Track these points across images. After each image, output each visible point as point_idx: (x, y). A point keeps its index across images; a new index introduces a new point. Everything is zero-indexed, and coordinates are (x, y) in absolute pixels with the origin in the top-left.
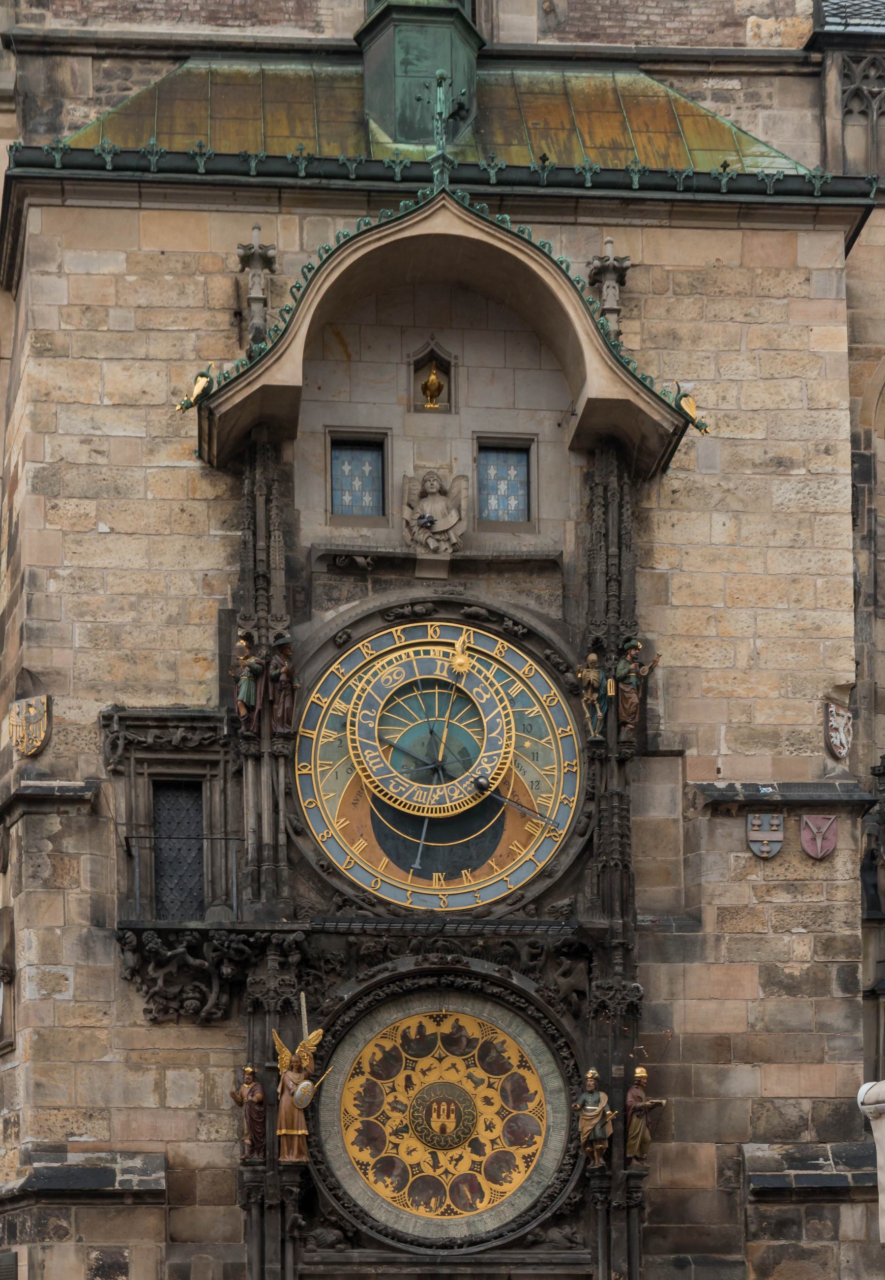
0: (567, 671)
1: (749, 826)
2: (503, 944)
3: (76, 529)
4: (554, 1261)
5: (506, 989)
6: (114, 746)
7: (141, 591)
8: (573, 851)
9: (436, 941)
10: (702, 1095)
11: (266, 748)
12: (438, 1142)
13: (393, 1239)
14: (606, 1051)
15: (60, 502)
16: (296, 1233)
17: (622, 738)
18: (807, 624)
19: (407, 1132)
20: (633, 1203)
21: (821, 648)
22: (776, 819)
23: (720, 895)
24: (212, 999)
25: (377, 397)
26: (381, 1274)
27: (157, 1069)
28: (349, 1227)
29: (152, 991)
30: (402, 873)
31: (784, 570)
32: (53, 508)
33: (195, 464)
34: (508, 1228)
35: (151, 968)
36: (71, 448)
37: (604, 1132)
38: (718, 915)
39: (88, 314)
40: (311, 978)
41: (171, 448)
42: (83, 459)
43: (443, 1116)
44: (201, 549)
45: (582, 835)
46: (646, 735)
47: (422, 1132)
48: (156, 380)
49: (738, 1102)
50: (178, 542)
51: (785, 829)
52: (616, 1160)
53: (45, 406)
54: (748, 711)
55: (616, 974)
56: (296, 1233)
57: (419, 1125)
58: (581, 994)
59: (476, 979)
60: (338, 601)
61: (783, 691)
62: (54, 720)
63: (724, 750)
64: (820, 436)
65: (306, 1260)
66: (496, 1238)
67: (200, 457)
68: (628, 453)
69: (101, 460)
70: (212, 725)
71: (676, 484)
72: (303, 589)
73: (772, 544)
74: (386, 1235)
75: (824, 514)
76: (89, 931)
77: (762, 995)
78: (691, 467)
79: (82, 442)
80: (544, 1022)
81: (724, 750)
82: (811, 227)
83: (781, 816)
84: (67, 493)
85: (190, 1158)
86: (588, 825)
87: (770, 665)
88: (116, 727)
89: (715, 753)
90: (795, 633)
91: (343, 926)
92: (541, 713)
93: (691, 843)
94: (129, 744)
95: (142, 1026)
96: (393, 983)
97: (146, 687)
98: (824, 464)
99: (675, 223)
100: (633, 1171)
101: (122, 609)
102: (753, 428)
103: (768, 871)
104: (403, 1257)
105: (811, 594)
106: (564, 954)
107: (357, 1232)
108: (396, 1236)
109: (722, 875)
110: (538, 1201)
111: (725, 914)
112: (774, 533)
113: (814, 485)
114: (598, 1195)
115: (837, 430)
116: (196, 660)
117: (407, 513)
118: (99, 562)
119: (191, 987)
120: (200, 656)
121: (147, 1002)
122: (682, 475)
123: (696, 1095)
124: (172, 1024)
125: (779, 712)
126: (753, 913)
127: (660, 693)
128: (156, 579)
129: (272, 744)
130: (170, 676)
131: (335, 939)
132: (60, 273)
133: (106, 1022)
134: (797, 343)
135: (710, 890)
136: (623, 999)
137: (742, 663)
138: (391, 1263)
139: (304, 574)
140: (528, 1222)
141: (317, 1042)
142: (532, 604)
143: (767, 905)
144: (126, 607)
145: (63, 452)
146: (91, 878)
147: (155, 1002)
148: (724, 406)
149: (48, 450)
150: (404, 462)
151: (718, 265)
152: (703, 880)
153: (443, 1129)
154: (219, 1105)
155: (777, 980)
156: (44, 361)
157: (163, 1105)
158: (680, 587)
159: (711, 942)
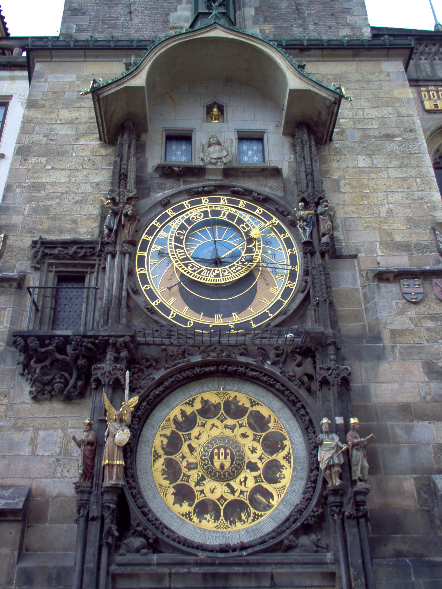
0: (288, 214)
1: (402, 286)
3: (36, 167)
4: (305, 561)
5: (261, 373)
6: (35, 256)
7: (63, 191)
8: (298, 301)
9: (216, 348)
12: (220, 476)
13: (184, 545)
15: (29, 158)
16: (110, 540)
17: (322, 252)
18: (416, 197)
19: (205, 479)
20: (360, 514)
22: (417, 282)
24: (72, 382)
25: (188, 117)
26: (175, 574)
27: (33, 430)
28: (150, 535)
30: (196, 314)
31: (398, 176)
32: (25, 160)
33: (97, 143)
34: (270, 536)
35: (32, 361)
38: (391, 334)
39: (56, 95)
40: (136, 370)
41: (87, 138)
42: (43, 142)
43: (222, 457)
44: (96, 174)
45: (303, 292)
46: (335, 249)
51: (424, 288)
53: (29, 125)
54: (390, 234)
55: (331, 360)
56: (110, 540)
57: (205, 464)
58: (310, 377)
59: (242, 367)
60: (164, 189)
61: (408, 226)
62: (7, 246)
63: (380, 253)
64: (406, 126)
65: (117, 562)
66: (261, 543)
67: (100, 139)
69: (52, 142)
70: (92, 246)
71: (337, 146)
72: (148, 188)
73: (390, 166)
74: (179, 542)
75: (415, 154)
76: (5, 349)
77: (426, 379)
79: (44, 136)
80: (287, 392)
81: (380, 253)
83: (420, 281)
85: (47, 489)
86: (306, 286)
87: (398, 215)
88: (38, 246)
89: (375, 255)
90: (410, 202)
91: (158, 340)
94: (45, 255)
95: (28, 403)
96: (188, 370)
97: (59, 230)
99: (324, 59)
101: (52, 198)
102: (372, 125)
103: (418, 310)
104: (191, 559)
106: (299, 353)
107: (157, 540)
108: (185, 542)
109: (390, 312)
110: (290, 515)
111: (394, 333)
112: (390, 162)
113: (407, 143)
114: (334, 508)
115: (414, 123)
116: (88, 219)
117: (201, 155)
118: (44, 180)
119: (59, 376)
121: (32, 387)
122: (341, 142)
124: (47, 402)
125: (408, 235)
127: (340, 229)
130: (73, 226)
131: (153, 347)
132: (46, 81)
133: (5, 401)
134: (388, 96)
135: (384, 321)
136: (338, 374)
137: (383, 215)
138: (182, 564)
140: (284, 531)
141: (134, 404)
142: (267, 190)
146: (11, 320)
147: (36, 386)
149: (27, 140)
150: (200, 138)
151: (346, 72)
152: (379, 315)
153: (222, 467)
155: (434, 370)
156: (32, 109)
157: (34, 453)
158: (345, 185)
159: (388, 349)
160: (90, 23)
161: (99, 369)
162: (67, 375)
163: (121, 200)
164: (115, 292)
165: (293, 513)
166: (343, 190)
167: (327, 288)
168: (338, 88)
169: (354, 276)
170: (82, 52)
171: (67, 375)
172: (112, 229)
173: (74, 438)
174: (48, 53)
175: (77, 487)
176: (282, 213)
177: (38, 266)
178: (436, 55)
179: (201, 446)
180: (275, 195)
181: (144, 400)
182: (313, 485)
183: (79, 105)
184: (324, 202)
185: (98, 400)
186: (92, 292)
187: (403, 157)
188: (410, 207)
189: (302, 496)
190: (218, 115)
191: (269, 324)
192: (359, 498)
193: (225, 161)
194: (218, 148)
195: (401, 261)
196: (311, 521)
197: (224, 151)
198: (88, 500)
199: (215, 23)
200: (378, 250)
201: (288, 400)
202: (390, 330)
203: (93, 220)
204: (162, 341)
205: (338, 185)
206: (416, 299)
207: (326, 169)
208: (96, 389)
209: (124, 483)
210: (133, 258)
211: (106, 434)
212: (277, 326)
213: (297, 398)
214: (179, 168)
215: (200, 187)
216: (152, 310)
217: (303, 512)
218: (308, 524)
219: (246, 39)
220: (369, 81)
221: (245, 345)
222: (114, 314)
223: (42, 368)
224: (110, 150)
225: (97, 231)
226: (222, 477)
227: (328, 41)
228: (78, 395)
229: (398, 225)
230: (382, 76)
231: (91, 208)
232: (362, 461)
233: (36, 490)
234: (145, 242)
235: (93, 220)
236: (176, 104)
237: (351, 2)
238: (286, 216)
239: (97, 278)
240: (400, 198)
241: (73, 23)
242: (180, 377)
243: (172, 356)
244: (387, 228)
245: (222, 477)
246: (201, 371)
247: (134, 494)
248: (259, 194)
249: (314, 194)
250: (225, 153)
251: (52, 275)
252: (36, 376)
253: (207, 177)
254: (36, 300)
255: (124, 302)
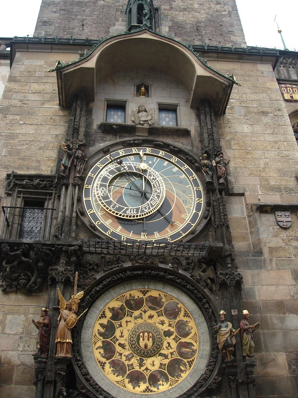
1: (277, 216)
2: (174, 258)
6: (9, 184)
7: (31, 140)
8: (203, 225)
10: (275, 329)
11: (71, 181)
12: (144, 353)
14: (227, 305)
18: (284, 155)
21: (290, 162)
22: (287, 213)
23: (269, 242)
24: (33, 279)
25: (124, 92)
29: (4, 275)
32: (4, 117)
33: (57, 107)
36: (14, 102)
37: (232, 342)
38: (269, 251)
39: (29, 73)
41: (50, 103)
43: (146, 339)
44: (56, 128)
45: (206, 218)
47: (135, 348)
48: (48, 87)
49: (292, 332)
50: (48, 127)
51: (292, 218)
52: (238, 357)
53: (9, 93)
54: (266, 180)
57: (133, 344)
58: (212, 280)
61: (279, 175)
63: (260, 193)
67: (60, 105)
68: (212, 102)
69: (25, 106)
71: (229, 117)
72: (93, 140)
73: (265, 133)
77: (295, 283)
78: (233, 113)
81: (260, 193)
82: (261, 62)
83: (289, 212)
84: (11, 114)
85: (13, 359)
87: (272, 167)
88: (11, 178)
90: (280, 158)
92: (186, 177)
93: (253, 224)
94: (16, 185)
96: (121, 273)
98: (279, 113)
99: (219, 60)
100: (248, 362)
101: (23, 145)
103: (287, 233)
105: (283, 147)
111: (272, 250)
112: (266, 130)
113: (276, 118)
116: (49, 160)
120: (50, 159)
121: (2, 282)
122: (230, 115)
123: (272, 329)
124: (13, 294)
125: (279, 181)
126: (284, 249)
128: (38, 137)
129: (74, 181)
130: (37, 164)
131: (95, 256)
132: (22, 64)
136: (234, 278)
137: (262, 166)
139: (94, 136)
143: (290, 246)
144: (25, 144)
145: (12, 104)
148: (242, 99)
150: (132, 107)
153: (146, 346)
154: (31, 333)
156: (12, 83)
159: (268, 261)
160: (54, 31)
161: (55, 270)
162: (29, 274)
163: (74, 147)
164: (67, 213)
165: (200, 381)
166: (233, 148)
167: (224, 216)
168: (231, 77)
169: (242, 208)
170: (49, 46)
171: (29, 274)
172: (67, 166)
173: (33, 321)
174: (25, 46)
175: (36, 357)
176: (191, 161)
177: (10, 192)
178: (290, 65)
179: (130, 331)
180: (186, 148)
181: (88, 294)
182: (214, 360)
183: (45, 81)
184: (220, 154)
185: (52, 293)
186: (50, 212)
187: (274, 128)
188: (280, 162)
189: (206, 368)
190: (145, 92)
191: (182, 241)
192: (249, 369)
193: (150, 123)
194: (144, 113)
195: (275, 199)
196: (214, 386)
197: (150, 116)
198: (44, 368)
199: (146, 29)
200: (259, 190)
201: (196, 297)
202: (269, 248)
203: (52, 161)
204: (102, 251)
205: (230, 145)
206: (286, 225)
207: (221, 133)
208: (51, 285)
209: (71, 356)
210: (81, 189)
211: (59, 319)
212: (188, 242)
213: (203, 295)
214: (117, 126)
215: (132, 140)
216: (94, 227)
217: (207, 380)
218: (211, 389)
219: (167, 41)
220: (250, 76)
221: (164, 255)
222: (66, 229)
223: (11, 268)
224: (66, 113)
225: (55, 169)
226: (146, 354)
227: (222, 48)
228: (37, 289)
229: (273, 174)
230: (258, 73)
231: (51, 152)
232: (250, 343)
233: (4, 359)
234: (91, 178)
235: (52, 161)
236: (115, 83)
237: (233, 28)
238: (193, 164)
239: (53, 203)
240: (273, 155)
241: (43, 30)
242: (115, 278)
243: (109, 262)
244: (265, 175)
245: (146, 354)
246: (131, 274)
247: (79, 365)
248: (174, 147)
249: (214, 149)
250: (150, 118)
251: (20, 200)
252: (6, 273)
253: (136, 134)
254: (8, 217)
255: (74, 221)
